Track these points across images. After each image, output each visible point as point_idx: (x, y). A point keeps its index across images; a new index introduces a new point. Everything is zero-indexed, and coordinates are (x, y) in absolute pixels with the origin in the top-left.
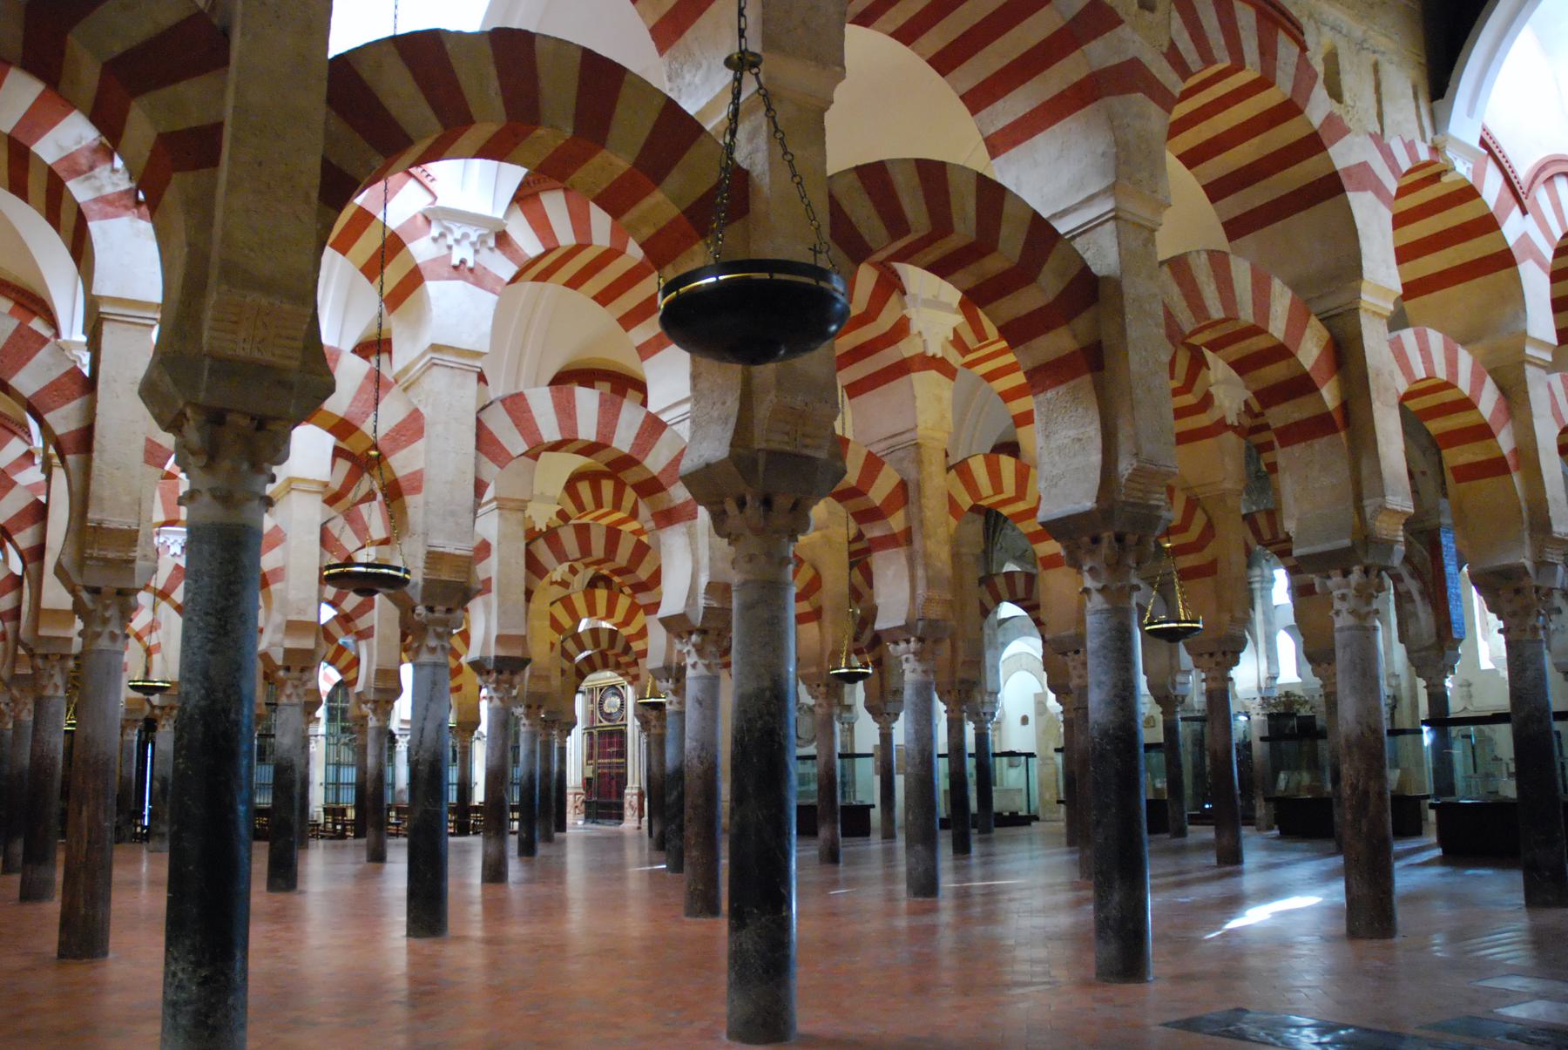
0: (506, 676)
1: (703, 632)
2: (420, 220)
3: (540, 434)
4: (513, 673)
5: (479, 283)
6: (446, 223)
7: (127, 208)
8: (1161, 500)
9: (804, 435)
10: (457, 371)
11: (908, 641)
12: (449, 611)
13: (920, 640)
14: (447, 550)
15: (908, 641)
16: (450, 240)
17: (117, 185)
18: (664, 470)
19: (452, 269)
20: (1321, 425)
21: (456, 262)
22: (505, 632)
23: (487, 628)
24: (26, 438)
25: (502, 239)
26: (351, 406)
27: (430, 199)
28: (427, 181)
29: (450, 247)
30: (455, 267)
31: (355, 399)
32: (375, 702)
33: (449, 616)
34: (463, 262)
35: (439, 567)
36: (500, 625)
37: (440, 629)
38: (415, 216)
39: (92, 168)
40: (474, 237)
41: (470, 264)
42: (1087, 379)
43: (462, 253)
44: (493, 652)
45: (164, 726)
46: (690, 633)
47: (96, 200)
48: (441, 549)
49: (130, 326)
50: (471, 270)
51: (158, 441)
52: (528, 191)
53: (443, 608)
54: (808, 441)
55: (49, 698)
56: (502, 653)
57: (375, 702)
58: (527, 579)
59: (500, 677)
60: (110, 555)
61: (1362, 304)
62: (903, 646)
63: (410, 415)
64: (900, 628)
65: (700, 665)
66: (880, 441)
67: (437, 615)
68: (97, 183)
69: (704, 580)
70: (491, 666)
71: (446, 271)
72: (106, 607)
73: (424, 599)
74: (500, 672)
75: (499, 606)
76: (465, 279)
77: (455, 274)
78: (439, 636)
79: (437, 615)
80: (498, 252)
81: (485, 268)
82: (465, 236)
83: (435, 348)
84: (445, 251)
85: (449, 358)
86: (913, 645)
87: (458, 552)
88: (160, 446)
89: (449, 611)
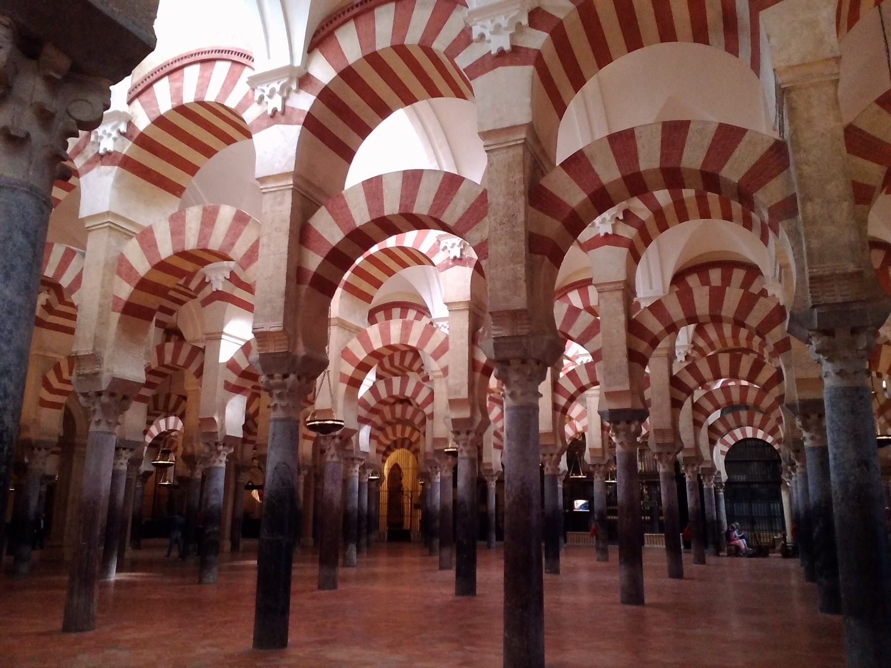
0: (621, 425)
3: (354, 222)
5: (289, 122)
6: (259, 87)
7: (97, 162)
10: (278, 193)
12: (285, 376)
14: (264, 330)
16: (266, 99)
17: (94, 151)
21: (270, 112)
24: (429, 315)
25: (304, 80)
26: (224, 241)
31: (227, 235)
32: (659, 454)
33: (286, 380)
34: (275, 111)
35: (266, 343)
37: (278, 392)
39: (84, 147)
40: (277, 87)
41: (279, 109)
43: (276, 103)
45: (596, 477)
47: (85, 165)
48: (261, 330)
49: (99, 231)
50: (283, 113)
51: (120, 296)
52: (323, 33)
53: (279, 375)
55: (329, 462)
56: (614, 406)
57: (659, 454)
60: (87, 371)
67: (276, 381)
68: (86, 154)
72: (94, 404)
73: (264, 370)
76: (279, 123)
77: (272, 121)
78: (280, 396)
79: (276, 381)
80: (302, 92)
81: (293, 108)
82: (272, 92)
87: (272, 330)
88: (120, 299)
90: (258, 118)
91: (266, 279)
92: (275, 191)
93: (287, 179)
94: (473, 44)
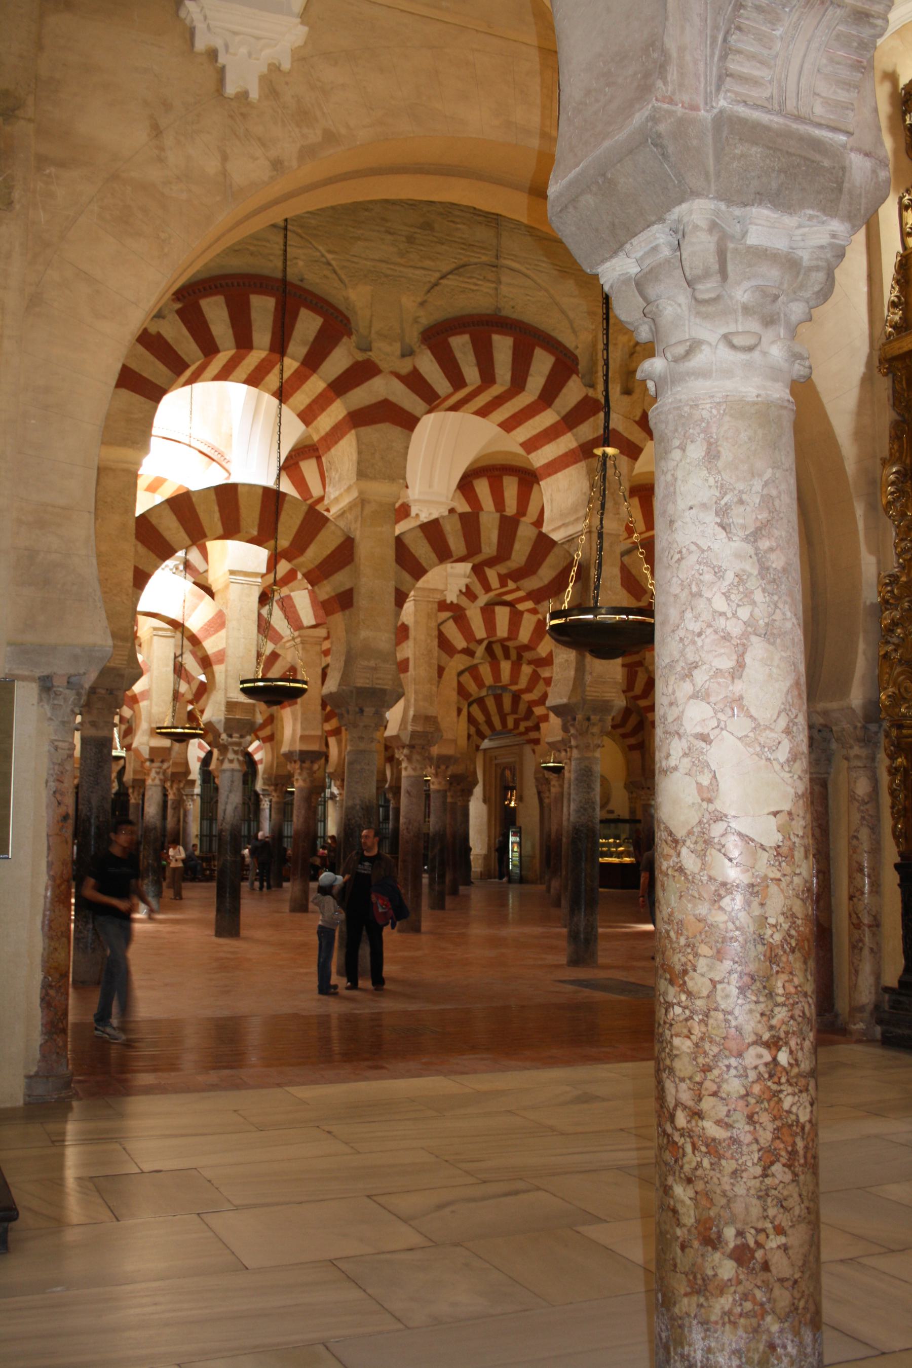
1: (412, 747)
4: (312, 762)
9: (378, 679)
22: (307, 733)
23: (294, 730)
27: (226, 475)
28: (224, 463)
36: (303, 729)
46: (403, 747)
54: (380, 681)
59: (304, 765)
62: (563, 754)
63: (217, 615)
65: (409, 769)
69: (411, 713)
70: (296, 758)
74: (303, 762)
75: (303, 714)
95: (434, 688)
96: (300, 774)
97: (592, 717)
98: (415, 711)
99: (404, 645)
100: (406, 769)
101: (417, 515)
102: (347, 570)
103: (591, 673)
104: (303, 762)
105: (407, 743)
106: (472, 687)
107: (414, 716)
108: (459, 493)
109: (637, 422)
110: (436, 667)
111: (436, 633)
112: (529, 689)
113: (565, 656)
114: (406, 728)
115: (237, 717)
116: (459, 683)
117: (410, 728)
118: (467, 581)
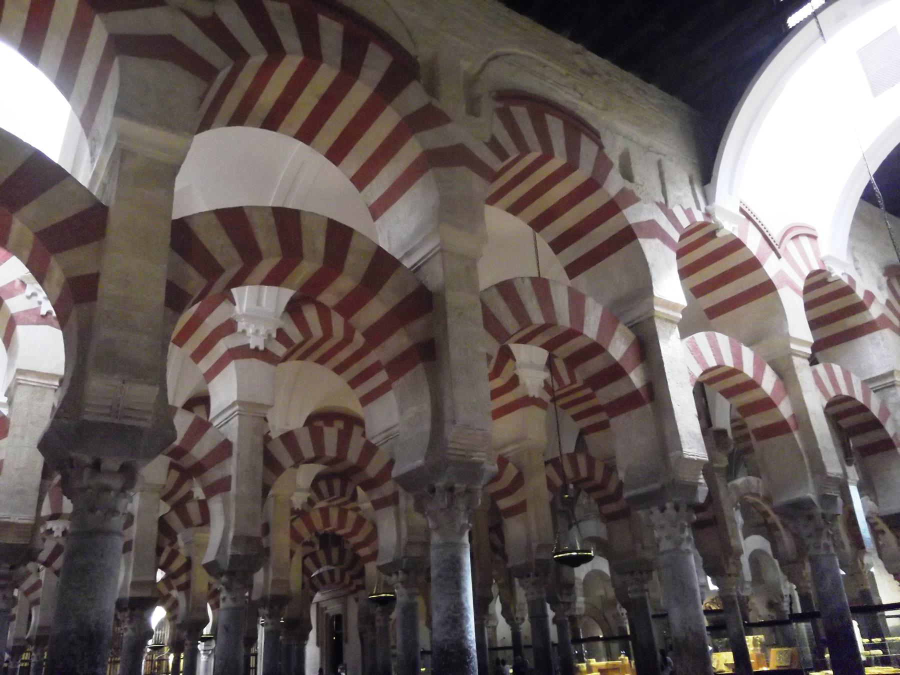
2: (18, 284)
8: (482, 457)
11: (397, 573)
12: (12, 568)
13: (406, 572)
14: (12, 520)
15: (397, 573)
18: (207, 456)
19: (40, 318)
20: (632, 401)
22: (140, 579)
23: (126, 577)
29: (40, 303)
30: (43, 316)
36: (134, 575)
38: (14, 282)
42: (420, 368)
44: (128, 594)
46: (222, 575)
56: (138, 594)
58: (159, 539)
61: (656, 313)
62: (394, 577)
64: (390, 564)
65: (228, 600)
66: (380, 434)
69: (231, 535)
71: (35, 320)
74: (133, 609)
83: (19, 372)
84: (36, 305)
85: (30, 379)
86: (401, 576)
89: (12, 568)
90: (26, 311)
91: (17, 469)
92: (34, 386)
93: (53, 379)
94: (236, 334)
95: (258, 507)
96: (130, 622)
97: (456, 486)
98: (235, 532)
99: (227, 462)
100: (224, 599)
101: (244, 332)
102: (93, 246)
103: (454, 422)
104: (133, 609)
105: (226, 568)
106: (306, 534)
107: (234, 537)
108: (287, 316)
109: (486, 144)
110: (260, 484)
111: (261, 448)
112: (354, 533)
113: (415, 409)
114: (225, 552)
115: (9, 542)
116: (292, 527)
117: (229, 552)
118: (308, 495)
